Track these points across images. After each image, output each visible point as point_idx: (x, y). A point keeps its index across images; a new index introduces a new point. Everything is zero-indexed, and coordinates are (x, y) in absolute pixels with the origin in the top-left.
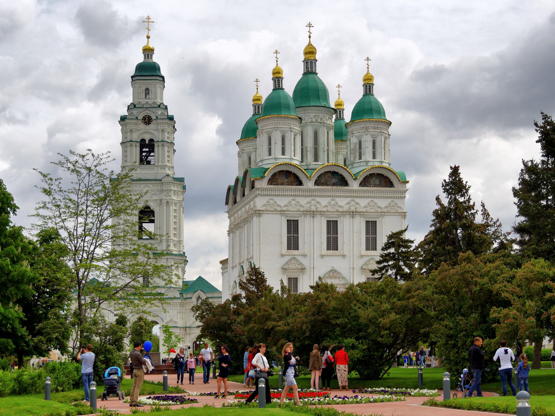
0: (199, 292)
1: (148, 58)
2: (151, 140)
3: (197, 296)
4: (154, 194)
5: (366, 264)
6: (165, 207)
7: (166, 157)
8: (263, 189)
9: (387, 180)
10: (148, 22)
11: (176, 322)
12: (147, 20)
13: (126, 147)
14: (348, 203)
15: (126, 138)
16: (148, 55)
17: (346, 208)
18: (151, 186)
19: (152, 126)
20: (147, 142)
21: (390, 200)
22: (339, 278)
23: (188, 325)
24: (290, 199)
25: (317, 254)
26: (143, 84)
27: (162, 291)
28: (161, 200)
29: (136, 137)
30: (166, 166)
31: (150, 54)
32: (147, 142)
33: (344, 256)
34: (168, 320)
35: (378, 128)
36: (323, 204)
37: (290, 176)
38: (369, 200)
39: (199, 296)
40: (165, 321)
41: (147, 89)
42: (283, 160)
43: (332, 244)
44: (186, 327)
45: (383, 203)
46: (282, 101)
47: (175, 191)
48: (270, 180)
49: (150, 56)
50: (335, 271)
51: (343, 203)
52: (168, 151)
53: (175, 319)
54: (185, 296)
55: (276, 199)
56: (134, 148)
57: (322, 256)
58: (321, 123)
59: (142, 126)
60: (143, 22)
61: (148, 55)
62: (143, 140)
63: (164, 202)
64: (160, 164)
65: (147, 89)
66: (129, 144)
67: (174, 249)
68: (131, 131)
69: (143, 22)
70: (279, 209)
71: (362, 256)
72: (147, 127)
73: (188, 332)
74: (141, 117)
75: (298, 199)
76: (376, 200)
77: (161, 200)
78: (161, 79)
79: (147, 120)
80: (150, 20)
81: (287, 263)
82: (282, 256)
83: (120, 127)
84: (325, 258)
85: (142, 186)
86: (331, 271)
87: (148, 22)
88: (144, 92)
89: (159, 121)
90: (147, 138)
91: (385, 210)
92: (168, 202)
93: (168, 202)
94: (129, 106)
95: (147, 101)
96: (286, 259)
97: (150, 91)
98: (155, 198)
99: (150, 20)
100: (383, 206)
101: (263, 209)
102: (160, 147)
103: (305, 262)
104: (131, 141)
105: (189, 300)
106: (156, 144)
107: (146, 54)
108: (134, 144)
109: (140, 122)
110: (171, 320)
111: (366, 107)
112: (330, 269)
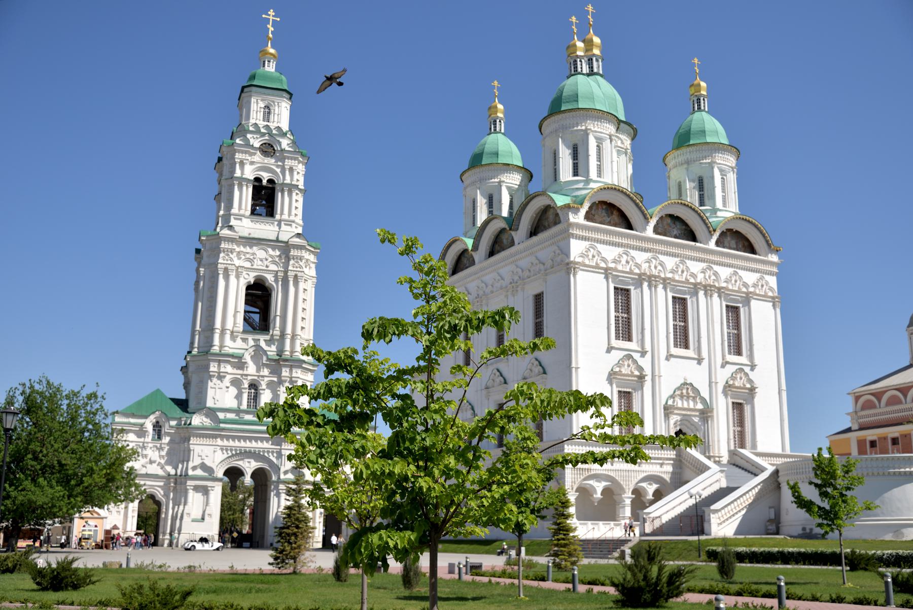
2: (270, 181)
4: (274, 262)
5: (733, 377)
8: (578, 226)
9: (746, 244)
14: (703, 272)
17: (700, 278)
18: (270, 250)
20: (265, 182)
21: (758, 275)
22: (694, 399)
24: (620, 250)
25: (663, 354)
30: (293, 222)
33: (700, 361)
36: (669, 267)
37: (612, 213)
38: (731, 270)
42: (610, 178)
43: (682, 338)
45: (750, 278)
47: (307, 260)
48: (587, 212)
50: (691, 384)
51: (696, 267)
55: (600, 247)
57: (669, 357)
59: (258, 157)
62: (258, 180)
65: (267, 107)
70: (603, 265)
71: (725, 364)
74: (257, 144)
75: (633, 253)
76: (741, 272)
81: (618, 364)
82: (610, 349)
84: (672, 359)
85: (255, 248)
86: (685, 384)
90: (265, 176)
91: (751, 289)
92: (296, 276)
93: (296, 276)
96: (617, 355)
98: (273, 267)
100: (750, 283)
101: (579, 260)
103: (645, 363)
106: (278, 188)
112: (682, 381)
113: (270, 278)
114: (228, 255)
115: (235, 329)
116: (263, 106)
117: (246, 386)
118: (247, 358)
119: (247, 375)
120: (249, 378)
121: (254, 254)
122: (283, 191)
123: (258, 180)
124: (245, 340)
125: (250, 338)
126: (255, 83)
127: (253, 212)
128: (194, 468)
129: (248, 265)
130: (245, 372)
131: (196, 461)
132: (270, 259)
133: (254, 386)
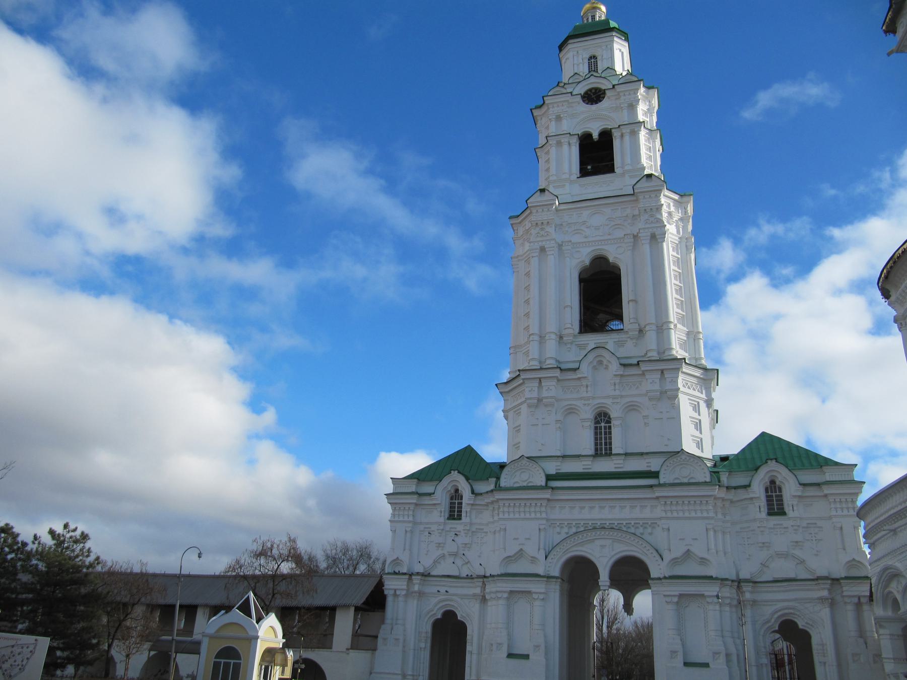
0: (772, 465)
3: (767, 480)
11: (703, 561)
13: (548, 153)
19: (605, 104)
20: (595, 136)
23: (744, 575)
27: (654, 464)
28: (635, 237)
34: (678, 552)
39: (773, 482)
40: (668, 557)
44: (739, 583)
53: (699, 550)
54: (724, 478)
56: (565, 147)
59: (584, 107)
64: (627, 168)
65: (593, 58)
72: (594, 107)
73: (748, 596)
77: (635, 237)
79: (594, 96)
85: (586, 213)
88: (586, 61)
89: (618, 88)
98: (619, 234)
102: (627, 138)
105: (742, 494)
106: (616, 134)
108: (564, 140)
109: (579, 98)
110: (688, 554)
113: (614, 255)
114: (542, 229)
115: (565, 332)
116: (588, 56)
117: (588, 414)
118: (585, 369)
119: (588, 399)
121: (584, 222)
122: (622, 136)
124: (581, 347)
125: (592, 340)
127: (584, 173)
128: (509, 559)
129: (576, 239)
131: (512, 550)
132: (613, 223)
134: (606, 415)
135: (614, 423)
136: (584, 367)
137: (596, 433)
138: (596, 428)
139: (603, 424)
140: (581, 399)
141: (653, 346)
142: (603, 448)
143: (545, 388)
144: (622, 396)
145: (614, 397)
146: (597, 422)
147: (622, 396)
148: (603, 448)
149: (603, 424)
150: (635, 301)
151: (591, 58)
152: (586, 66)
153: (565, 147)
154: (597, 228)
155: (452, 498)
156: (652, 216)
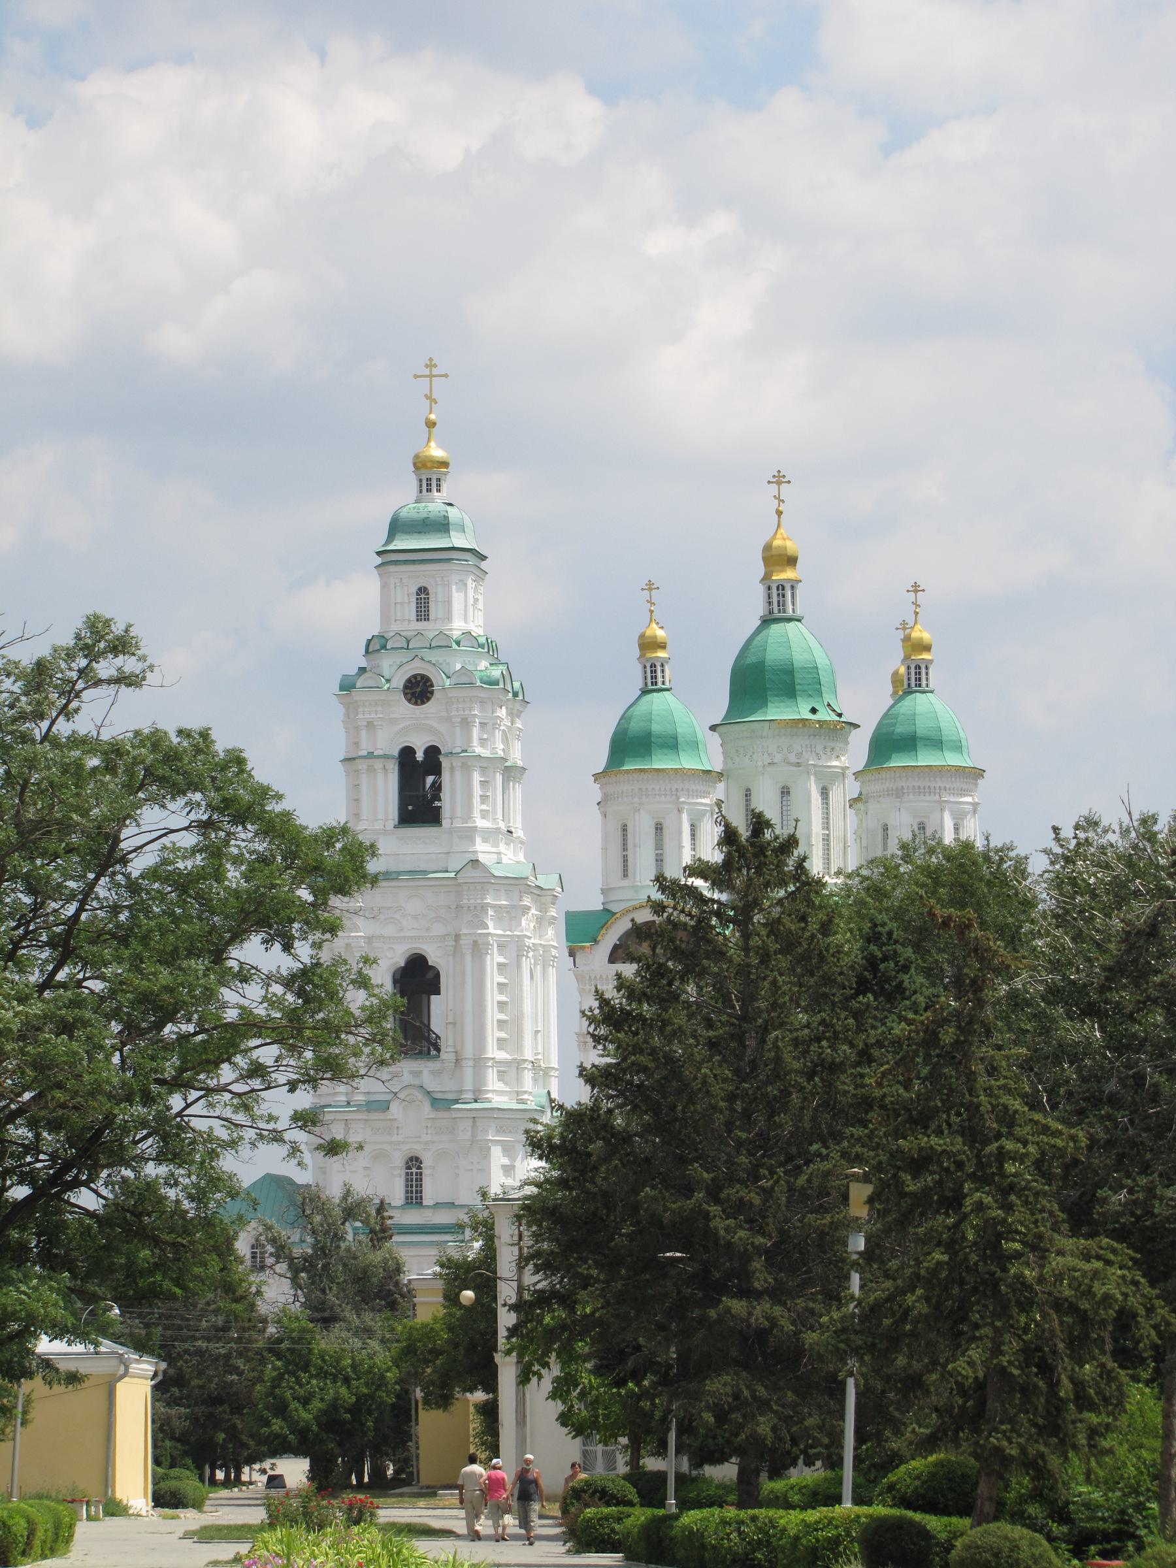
1: (429, 490)
2: (433, 752)
6: (468, 958)
7: (476, 800)
10: (431, 376)
12: (427, 372)
15: (357, 744)
16: (429, 480)
20: (420, 756)
26: (408, 580)
28: (457, 937)
29: (388, 743)
31: (434, 477)
32: (420, 756)
35: (929, 791)
41: (423, 590)
46: (656, 728)
49: (434, 483)
52: (484, 783)
56: (380, 776)
58: (798, 765)
59: (404, 708)
60: (416, 377)
61: (429, 480)
62: (407, 753)
63: (465, 942)
65: (423, 590)
66: (362, 765)
67: (500, 1086)
68: (370, 725)
69: (416, 377)
78: (468, 556)
79: (419, 690)
80: (435, 371)
83: (342, 710)
87: (431, 376)
92: (475, 943)
93: (475, 943)
94: (369, 641)
95: (422, 625)
97: (432, 596)
98: (438, 929)
99: (435, 371)
102: (458, 774)
104: (371, 755)
107: (424, 478)
108: (378, 764)
111: (900, 729)
116: (414, 590)
117: (399, 1161)
119: (399, 1143)
120: (405, 1147)
122: (452, 768)
123: (407, 753)
126: (391, 547)
129: (390, 931)
130: (395, 1138)
133: (414, 1163)
134: (417, 1159)
135: (425, 1171)
136: (395, 1108)
137: (407, 1180)
138: (407, 1174)
139: (414, 1170)
140: (391, 1143)
141: (468, 1086)
142: (414, 1196)
143: (351, 1131)
144: (433, 1142)
145: (426, 1143)
146: (409, 1168)
147: (433, 1142)
148: (414, 1196)
149: (414, 1170)
150: (454, 1024)
151: (420, 589)
152: (414, 605)
153: (380, 776)
154: (415, 917)
155: (253, 1247)
156: (476, 916)
